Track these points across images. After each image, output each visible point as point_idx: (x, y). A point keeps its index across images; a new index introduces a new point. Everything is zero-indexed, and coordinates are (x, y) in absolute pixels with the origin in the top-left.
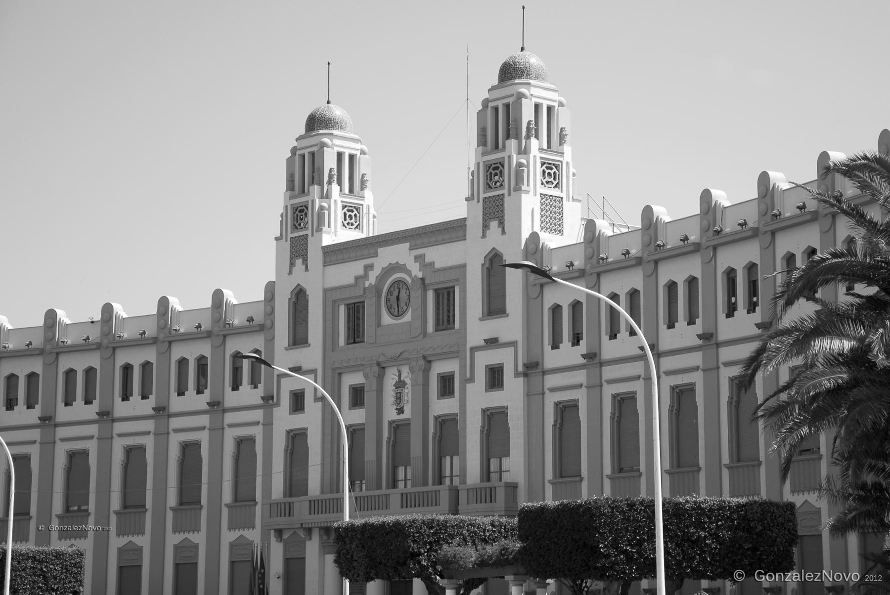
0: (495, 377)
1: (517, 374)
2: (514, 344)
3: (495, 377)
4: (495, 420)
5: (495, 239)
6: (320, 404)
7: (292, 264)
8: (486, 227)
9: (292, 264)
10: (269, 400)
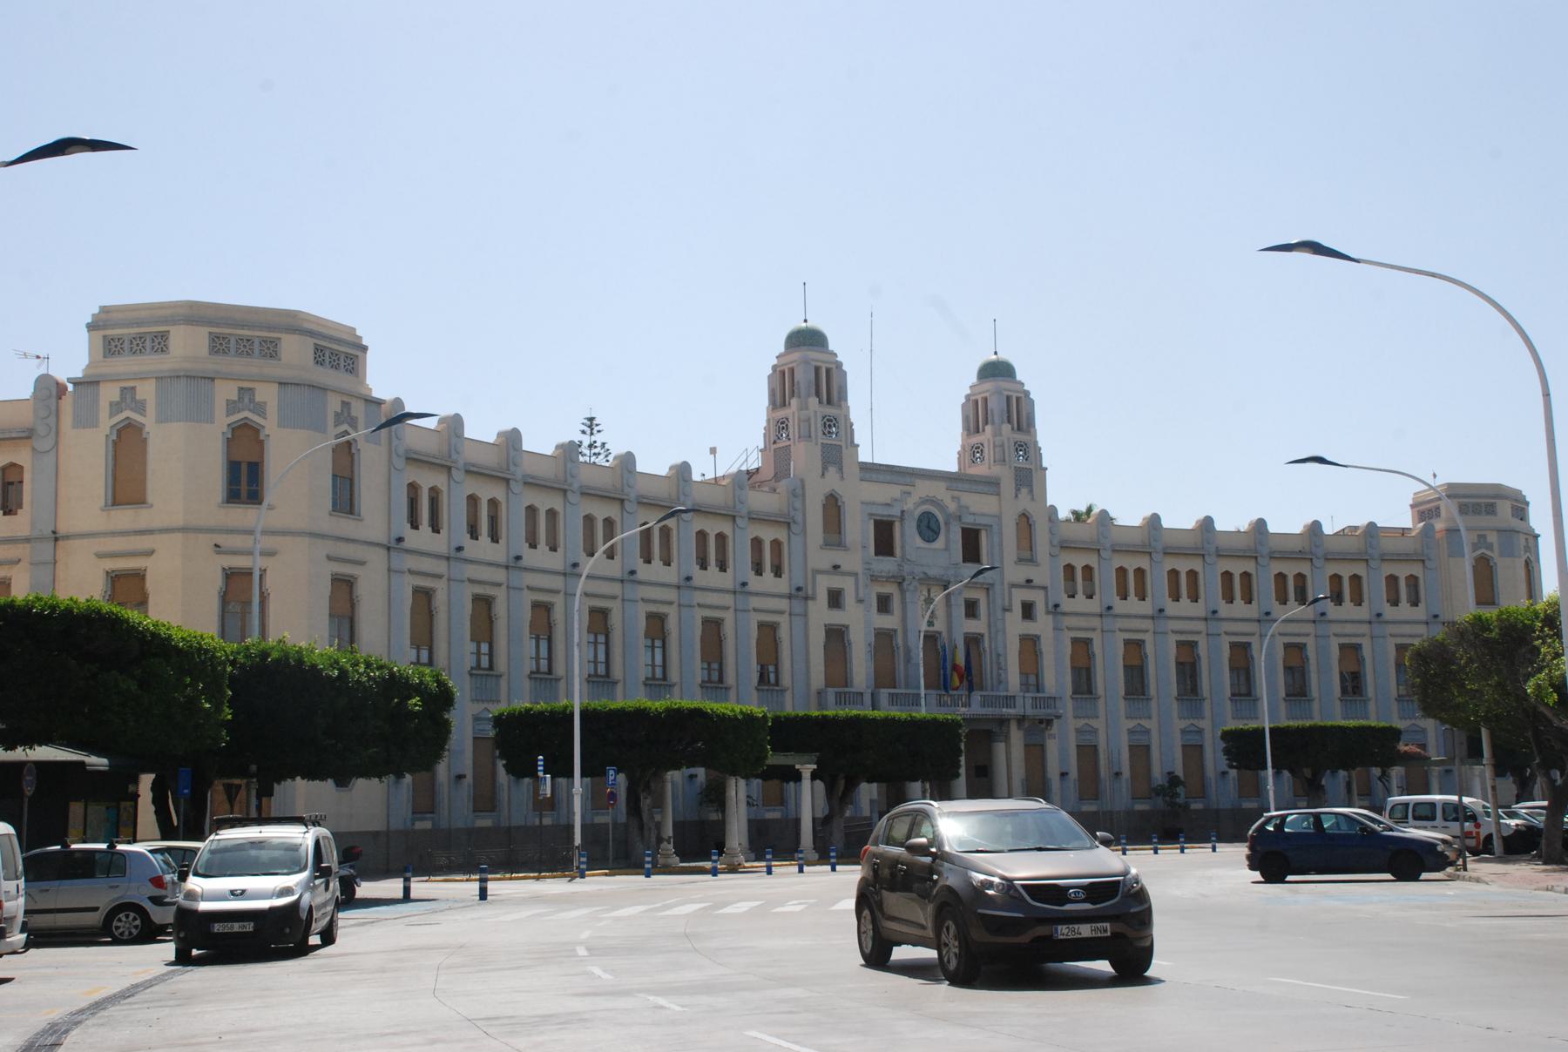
0: (1028, 611)
1: (1048, 612)
2: (1045, 588)
3: (1028, 611)
4: (1030, 644)
5: (1024, 503)
6: (861, 606)
7: (825, 469)
8: (1018, 490)
9: (825, 469)
10: (800, 594)
